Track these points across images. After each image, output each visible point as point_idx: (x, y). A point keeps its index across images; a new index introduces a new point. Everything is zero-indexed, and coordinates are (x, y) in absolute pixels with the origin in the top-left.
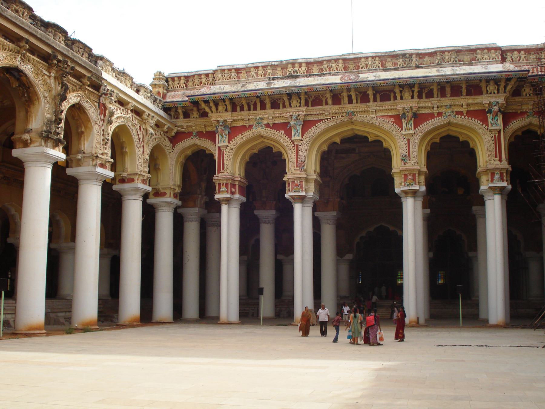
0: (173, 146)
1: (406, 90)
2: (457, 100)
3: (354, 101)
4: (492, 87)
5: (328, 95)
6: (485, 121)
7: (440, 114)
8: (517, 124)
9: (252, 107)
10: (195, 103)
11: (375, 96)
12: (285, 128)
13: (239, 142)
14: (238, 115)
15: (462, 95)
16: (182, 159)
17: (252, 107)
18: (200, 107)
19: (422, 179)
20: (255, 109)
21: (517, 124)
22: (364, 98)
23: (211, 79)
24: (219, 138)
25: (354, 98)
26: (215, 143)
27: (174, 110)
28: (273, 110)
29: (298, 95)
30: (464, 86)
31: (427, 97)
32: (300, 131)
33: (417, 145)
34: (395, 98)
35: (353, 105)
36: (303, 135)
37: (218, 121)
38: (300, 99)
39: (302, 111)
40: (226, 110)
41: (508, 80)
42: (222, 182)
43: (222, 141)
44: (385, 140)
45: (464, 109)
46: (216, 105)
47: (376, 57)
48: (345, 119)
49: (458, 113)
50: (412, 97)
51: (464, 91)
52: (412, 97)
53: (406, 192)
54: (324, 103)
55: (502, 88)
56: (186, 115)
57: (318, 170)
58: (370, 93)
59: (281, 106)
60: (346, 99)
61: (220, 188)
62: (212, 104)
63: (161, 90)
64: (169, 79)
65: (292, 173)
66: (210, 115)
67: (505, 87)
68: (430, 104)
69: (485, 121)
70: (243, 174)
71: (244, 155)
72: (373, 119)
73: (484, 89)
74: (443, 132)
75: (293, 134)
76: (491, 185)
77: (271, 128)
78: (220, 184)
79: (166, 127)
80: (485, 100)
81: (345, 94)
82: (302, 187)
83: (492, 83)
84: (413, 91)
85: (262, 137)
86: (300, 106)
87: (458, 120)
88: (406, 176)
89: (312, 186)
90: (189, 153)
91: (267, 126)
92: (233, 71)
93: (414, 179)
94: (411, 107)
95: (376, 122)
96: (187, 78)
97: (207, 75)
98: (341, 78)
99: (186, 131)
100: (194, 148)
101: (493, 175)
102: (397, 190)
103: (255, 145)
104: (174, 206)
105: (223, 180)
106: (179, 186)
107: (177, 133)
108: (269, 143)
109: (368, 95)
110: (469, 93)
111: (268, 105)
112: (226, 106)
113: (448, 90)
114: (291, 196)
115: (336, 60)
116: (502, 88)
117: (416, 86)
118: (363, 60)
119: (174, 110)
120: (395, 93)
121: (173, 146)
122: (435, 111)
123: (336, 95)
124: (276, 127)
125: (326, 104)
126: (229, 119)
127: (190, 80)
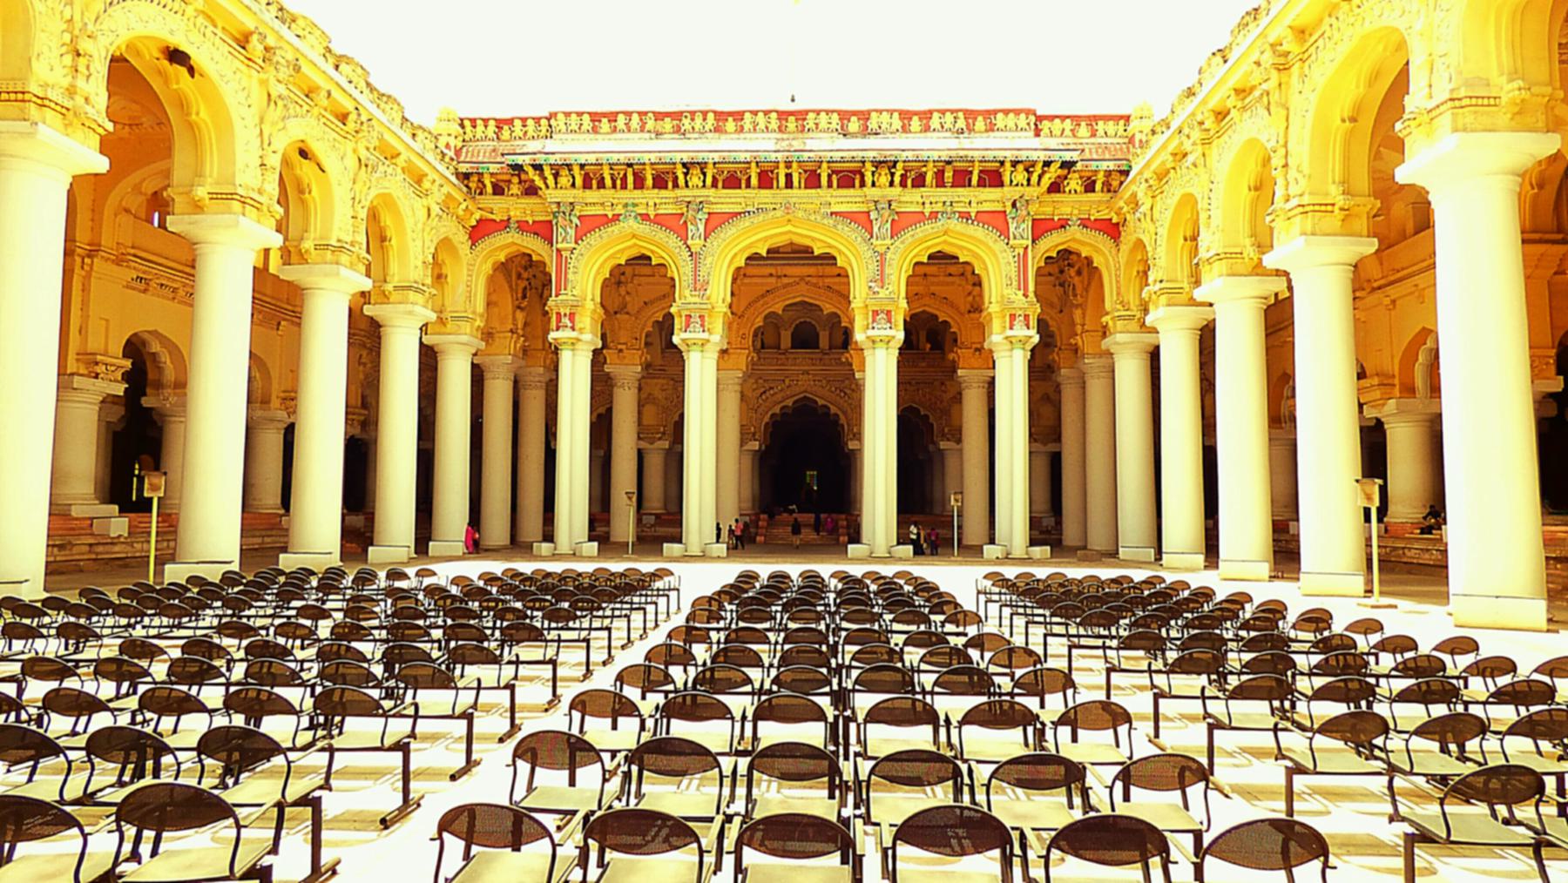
1: (885, 171)
3: (796, 183)
4: (1021, 176)
10: (518, 168)
11: (829, 176)
12: (675, 224)
14: (593, 195)
16: (487, 268)
18: (523, 177)
19: (899, 319)
20: (624, 187)
21: (1052, 243)
22: (813, 181)
23: (544, 128)
24: (559, 232)
26: (550, 241)
27: (475, 178)
29: (702, 166)
31: (913, 186)
32: (702, 228)
34: (863, 184)
35: (795, 191)
38: (704, 174)
41: (1047, 164)
43: (565, 237)
44: (840, 252)
45: (973, 210)
46: (556, 176)
49: (965, 216)
50: (892, 184)
51: (975, 180)
52: (892, 184)
55: (1035, 178)
56: (498, 190)
57: (729, 299)
61: (559, 320)
62: (548, 172)
63: (453, 142)
64: (467, 123)
65: (684, 301)
66: (544, 192)
67: (1040, 177)
69: (1004, 232)
70: (598, 300)
71: (602, 266)
72: (810, 219)
73: (1006, 180)
76: (1009, 333)
78: (558, 314)
79: (463, 206)
80: (1008, 193)
81: (782, 172)
84: (892, 175)
85: (634, 236)
88: (876, 313)
91: (645, 217)
96: (501, 123)
97: (537, 120)
100: (514, 249)
101: (1013, 317)
102: (859, 336)
103: (622, 251)
106: (481, 316)
108: (646, 248)
110: (981, 184)
111: (649, 182)
113: (949, 175)
115: (766, 113)
116: (1035, 178)
117: (900, 165)
118: (811, 116)
119: (475, 178)
120: (863, 176)
122: (927, 210)
124: (660, 221)
125: (748, 186)
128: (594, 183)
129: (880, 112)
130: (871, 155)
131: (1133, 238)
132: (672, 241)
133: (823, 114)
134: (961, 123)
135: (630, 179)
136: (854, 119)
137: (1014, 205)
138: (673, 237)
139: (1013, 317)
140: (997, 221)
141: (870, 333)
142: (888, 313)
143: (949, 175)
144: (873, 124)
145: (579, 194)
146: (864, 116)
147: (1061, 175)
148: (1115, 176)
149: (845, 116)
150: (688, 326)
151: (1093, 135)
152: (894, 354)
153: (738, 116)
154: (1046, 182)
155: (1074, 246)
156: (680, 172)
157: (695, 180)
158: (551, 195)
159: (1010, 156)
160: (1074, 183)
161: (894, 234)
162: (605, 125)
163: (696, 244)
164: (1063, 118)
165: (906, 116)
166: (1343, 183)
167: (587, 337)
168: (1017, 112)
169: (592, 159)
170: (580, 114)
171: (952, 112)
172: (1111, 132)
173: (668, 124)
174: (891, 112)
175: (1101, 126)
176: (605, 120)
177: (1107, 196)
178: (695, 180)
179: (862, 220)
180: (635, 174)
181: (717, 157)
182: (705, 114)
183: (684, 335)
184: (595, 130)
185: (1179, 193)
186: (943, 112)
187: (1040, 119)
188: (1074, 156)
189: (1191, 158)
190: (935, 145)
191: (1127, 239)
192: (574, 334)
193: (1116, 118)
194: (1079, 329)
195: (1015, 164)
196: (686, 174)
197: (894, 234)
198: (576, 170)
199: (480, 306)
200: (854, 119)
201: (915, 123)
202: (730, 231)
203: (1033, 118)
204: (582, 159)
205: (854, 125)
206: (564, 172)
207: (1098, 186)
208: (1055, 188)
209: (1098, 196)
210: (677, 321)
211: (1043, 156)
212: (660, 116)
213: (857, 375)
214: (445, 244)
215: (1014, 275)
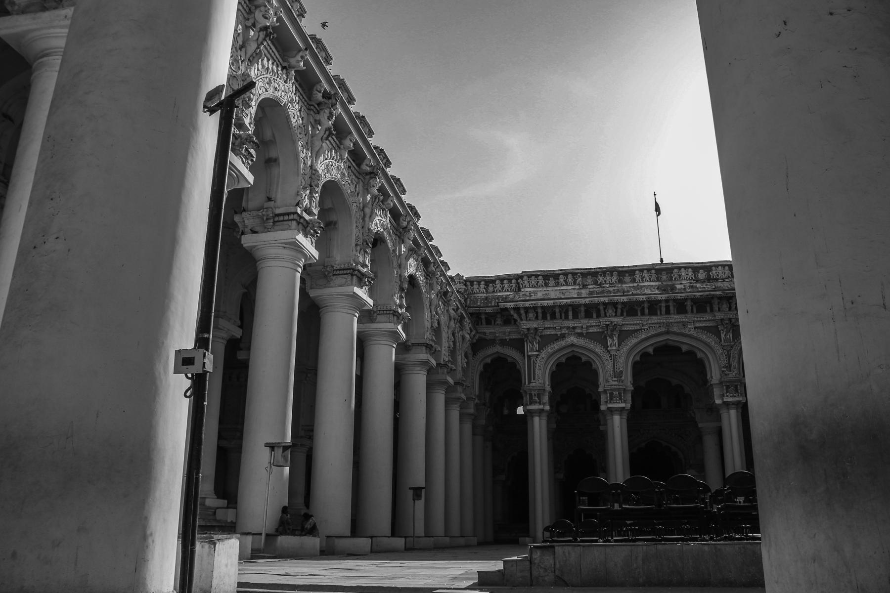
0: (474, 354)
3: (672, 311)
5: (646, 305)
9: (563, 315)
12: (601, 338)
14: (548, 324)
16: (481, 368)
17: (563, 315)
20: (567, 318)
23: (514, 285)
24: (528, 346)
25: (672, 308)
26: (522, 352)
32: (616, 341)
34: (712, 310)
35: (672, 316)
37: (528, 329)
38: (616, 308)
39: (618, 320)
40: (537, 318)
42: (533, 393)
43: (531, 348)
46: (526, 313)
47: (689, 267)
48: (663, 330)
53: (727, 405)
54: (639, 314)
56: (488, 322)
58: (689, 303)
60: (664, 309)
62: (522, 312)
77: (585, 337)
78: (530, 395)
81: (663, 305)
85: (572, 345)
86: (616, 316)
88: (728, 387)
89: (629, 397)
90: (489, 360)
92: (540, 277)
93: (737, 391)
94: (730, 320)
95: (693, 333)
96: (489, 282)
97: (510, 280)
100: (496, 356)
102: (718, 401)
107: (480, 340)
109: (685, 306)
111: (583, 314)
112: (537, 313)
114: (608, 408)
118: (676, 270)
121: (474, 354)
123: (653, 307)
124: (589, 336)
130: (718, 293)
132: (599, 349)
133: (683, 270)
135: (570, 314)
141: (726, 399)
142: (736, 386)
144: (714, 273)
150: (611, 399)
152: (740, 410)
156: (601, 308)
157: (610, 311)
158: (525, 325)
162: (552, 282)
167: (547, 408)
170: (537, 276)
173: (589, 280)
178: (610, 311)
180: (573, 310)
183: (610, 405)
184: (546, 285)
192: (541, 407)
196: (605, 309)
198: (540, 311)
200: (701, 271)
213: (700, 425)
214: (466, 356)
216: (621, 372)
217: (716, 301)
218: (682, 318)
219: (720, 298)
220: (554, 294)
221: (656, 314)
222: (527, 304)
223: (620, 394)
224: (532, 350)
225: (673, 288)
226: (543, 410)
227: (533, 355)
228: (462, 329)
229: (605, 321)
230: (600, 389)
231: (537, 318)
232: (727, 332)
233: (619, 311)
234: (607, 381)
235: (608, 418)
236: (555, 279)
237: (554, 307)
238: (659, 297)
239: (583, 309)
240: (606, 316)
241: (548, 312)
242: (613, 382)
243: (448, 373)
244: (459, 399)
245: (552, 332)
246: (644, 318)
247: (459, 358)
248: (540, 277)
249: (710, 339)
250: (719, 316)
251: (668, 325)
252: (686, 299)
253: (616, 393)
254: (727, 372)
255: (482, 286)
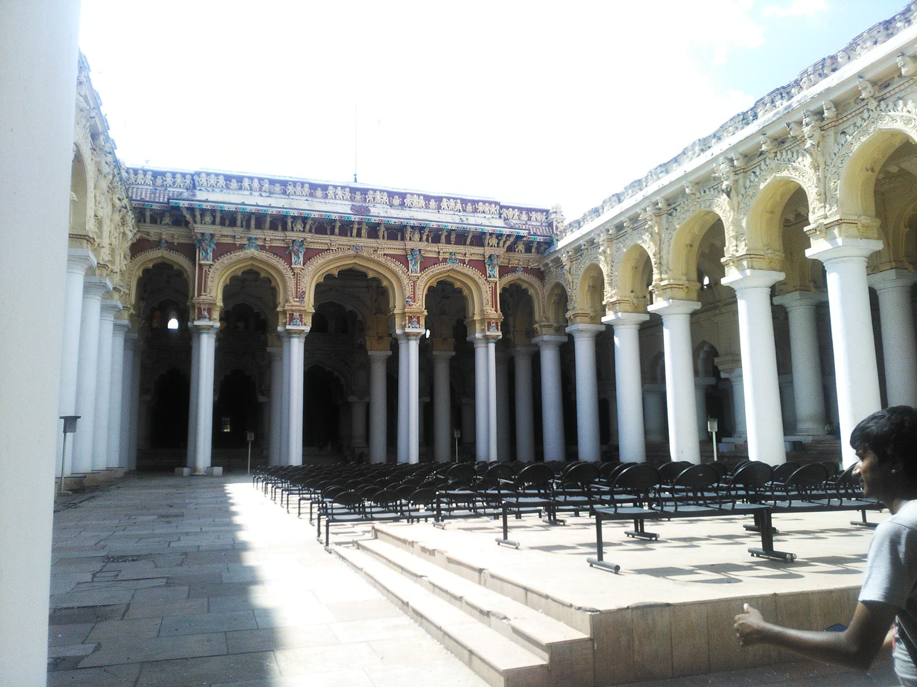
1: (417, 232)
2: (461, 249)
4: (494, 241)
5: (338, 225)
6: (484, 272)
7: (445, 260)
8: (509, 278)
12: (285, 253)
13: (226, 262)
14: (228, 231)
15: (465, 244)
17: (244, 223)
21: (509, 278)
23: (188, 182)
25: (364, 232)
26: (192, 258)
28: (272, 232)
29: (304, 220)
30: (470, 236)
32: (301, 259)
33: (422, 288)
34: (403, 239)
35: (363, 239)
36: (304, 264)
37: (203, 234)
38: (305, 224)
41: (509, 236)
42: (202, 307)
43: (205, 258)
46: (202, 215)
48: (351, 252)
49: (463, 262)
50: (421, 240)
56: (154, 221)
58: (382, 228)
59: (280, 228)
60: (355, 231)
62: (198, 214)
64: (131, 171)
68: (436, 250)
69: (484, 272)
74: (441, 277)
75: (293, 260)
77: (267, 250)
78: (200, 309)
81: (356, 226)
82: (301, 321)
83: (494, 236)
84: (421, 234)
85: (253, 258)
86: (304, 231)
87: (459, 267)
88: (410, 318)
89: (308, 320)
93: (418, 323)
98: (353, 208)
99: (151, 239)
100: (159, 261)
101: (489, 324)
102: (398, 331)
104: (126, 329)
105: (205, 304)
110: (472, 244)
111: (268, 225)
112: (214, 217)
113: (453, 237)
115: (343, 188)
118: (371, 192)
122: (441, 257)
123: (345, 228)
126: (218, 233)
127: (159, 177)
128: (227, 222)
129: (412, 194)
131: (553, 282)
132: (281, 265)
133: (378, 193)
134: (459, 206)
135: (253, 222)
136: (396, 197)
137: (490, 257)
138: (282, 261)
139: (489, 324)
140: (480, 265)
141: (407, 330)
142: (418, 318)
143: (453, 237)
144: (407, 201)
145: (217, 230)
146: (403, 196)
147: (514, 243)
148: (544, 246)
149: (391, 194)
151: (530, 219)
152: (418, 342)
153: (325, 188)
154: (508, 243)
155: (519, 282)
156: (289, 221)
159: (490, 230)
160: (521, 247)
161: (423, 268)
163: (298, 266)
164: (514, 208)
165: (427, 198)
166: (686, 275)
167: (217, 324)
168: (490, 203)
169: (232, 208)
170: (217, 175)
171: (454, 199)
172: (539, 218)
174: (419, 195)
175: (533, 215)
176: (234, 181)
177: (538, 256)
178: (299, 226)
179: (403, 260)
181: (316, 215)
182: (303, 184)
183: (288, 327)
184: (228, 187)
185: (588, 263)
186: (449, 198)
187: (502, 207)
188: (523, 233)
189: (602, 248)
190: (448, 218)
191: (550, 283)
192: (211, 323)
193: (542, 211)
194: (512, 329)
195: (491, 234)
196: (292, 222)
197: (423, 268)
198: (218, 215)
199: (133, 301)
200: (396, 197)
201: (433, 203)
202: (318, 261)
203: (498, 207)
204: (226, 207)
205: (397, 201)
206: (209, 214)
207: (533, 250)
208: (511, 249)
209: (533, 255)
210: (281, 317)
211: (506, 231)
212: (272, 182)
213: (370, 353)
215: (490, 300)
216: (304, 293)
217: (409, 230)
218: (372, 242)
219: (413, 227)
220: (231, 199)
221: (346, 235)
222: (205, 206)
223: (301, 315)
224: (206, 258)
225: (367, 210)
226: (212, 326)
227: (206, 265)
228: (123, 225)
229: (291, 235)
230: (279, 309)
231: (214, 223)
232: (416, 264)
233: (308, 227)
234: (287, 301)
235: (285, 340)
236: (238, 182)
237: (235, 213)
238: (353, 218)
239: (268, 219)
240: (293, 230)
241: (229, 218)
242: (294, 303)
243: (107, 275)
244: (115, 307)
245: (230, 241)
246: (332, 237)
247: (117, 258)
248: (222, 177)
249: (398, 268)
250: (410, 245)
251: (356, 248)
252: (379, 224)
253: (296, 315)
254: (411, 303)
255: (149, 176)
